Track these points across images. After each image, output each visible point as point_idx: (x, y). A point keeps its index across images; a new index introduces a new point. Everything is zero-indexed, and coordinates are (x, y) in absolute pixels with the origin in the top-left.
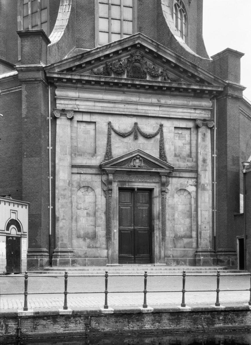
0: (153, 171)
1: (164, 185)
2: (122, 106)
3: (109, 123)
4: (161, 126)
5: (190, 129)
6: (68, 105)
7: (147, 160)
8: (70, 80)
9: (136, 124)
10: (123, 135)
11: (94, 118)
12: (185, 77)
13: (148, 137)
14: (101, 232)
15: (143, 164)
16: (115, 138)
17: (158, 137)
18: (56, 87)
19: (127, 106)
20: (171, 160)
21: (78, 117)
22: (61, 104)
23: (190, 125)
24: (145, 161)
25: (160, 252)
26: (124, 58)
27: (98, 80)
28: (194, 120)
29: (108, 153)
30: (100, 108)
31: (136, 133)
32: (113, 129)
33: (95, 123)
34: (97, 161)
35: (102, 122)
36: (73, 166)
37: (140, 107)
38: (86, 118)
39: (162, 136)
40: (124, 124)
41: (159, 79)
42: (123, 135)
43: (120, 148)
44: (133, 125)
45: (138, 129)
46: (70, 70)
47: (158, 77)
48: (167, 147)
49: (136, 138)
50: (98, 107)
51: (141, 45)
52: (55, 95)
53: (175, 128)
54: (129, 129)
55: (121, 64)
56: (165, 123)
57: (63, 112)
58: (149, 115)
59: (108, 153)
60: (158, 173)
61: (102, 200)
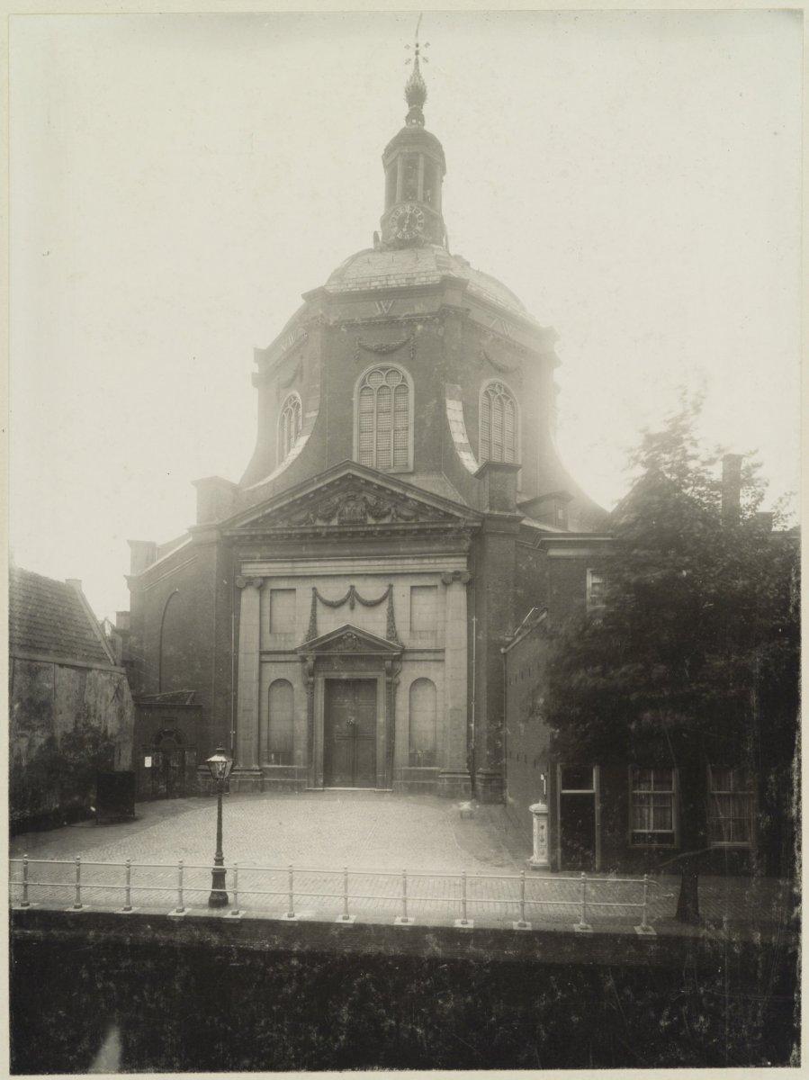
1: (390, 672)
3: (314, 589)
5: (436, 587)
13: (372, 605)
16: (320, 609)
17: (384, 607)
23: (436, 581)
31: (352, 599)
32: (318, 596)
33: (294, 590)
35: (304, 590)
39: (391, 603)
40: (334, 591)
41: (387, 520)
43: (329, 624)
44: (349, 589)
45: (357, 596)
47: (384, 516)
49: (352, 608)
57: (250, 582)
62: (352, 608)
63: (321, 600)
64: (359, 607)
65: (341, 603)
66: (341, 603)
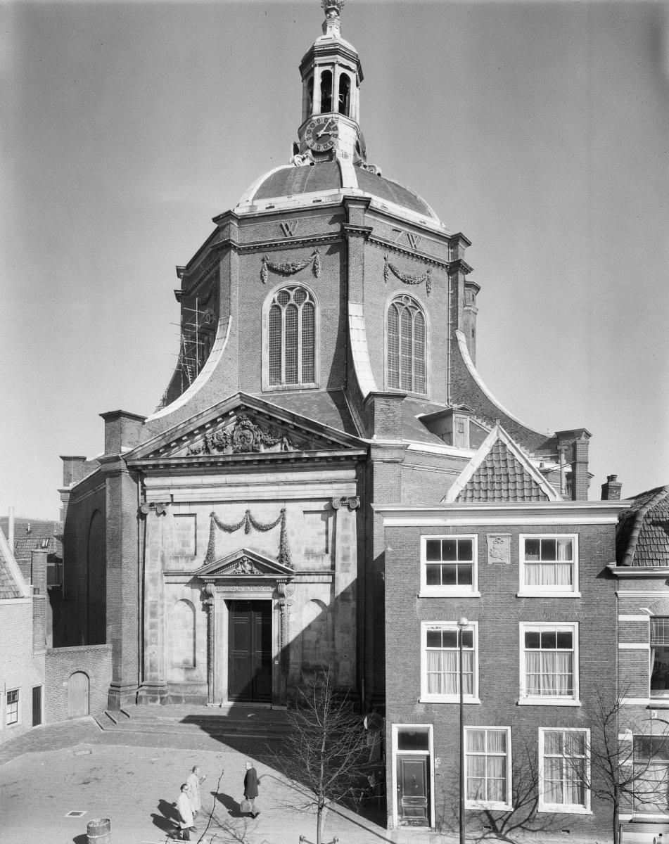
0: (266, 577)
2: (228, 489)
3: (212, 515)
4: (283, 511)
6: (163, 496)
7: (260, 563)
8: (155, 466)
9: (248, 512)
10: (229, 529)
11: (194, 509)
12: (313, 440)
14: (202, 659)
15: (254, 568)
17: (279, 526)
18: (146, 475)
19: (233, 489)
20: (298, 560)
21: (171, 510)
22: (152, 496)
24: (254, 563)
25: (279, 688)
26: (228, 426)
27: (189, 462)
28: (330, 499)
29: (210, 554)
30: (199, 496)
33: (194, 515)
34: (197, 564)
35: (204, 512)
36: (167, 574)
37: (251, 489)
38: (184, 509)
39: (283, 524)
40: (231, 514)
42: (229, 529)
43: (227, 546)
46: (156, 452)
48: (291, 541)
50: (197, 495)
51: (246, 407)
52: (145, 486)
53: (305, 512)
54: (240, 520)
55: (225, 434)
56: (289, 506)
58: (265, 498)
59: (210, 554)
60: (275, 580)
61: (202, 616)
62: (247, 532)
63: (220, 525)
64: (253, 531)
65: (238, 526)
66: (238, 526)
